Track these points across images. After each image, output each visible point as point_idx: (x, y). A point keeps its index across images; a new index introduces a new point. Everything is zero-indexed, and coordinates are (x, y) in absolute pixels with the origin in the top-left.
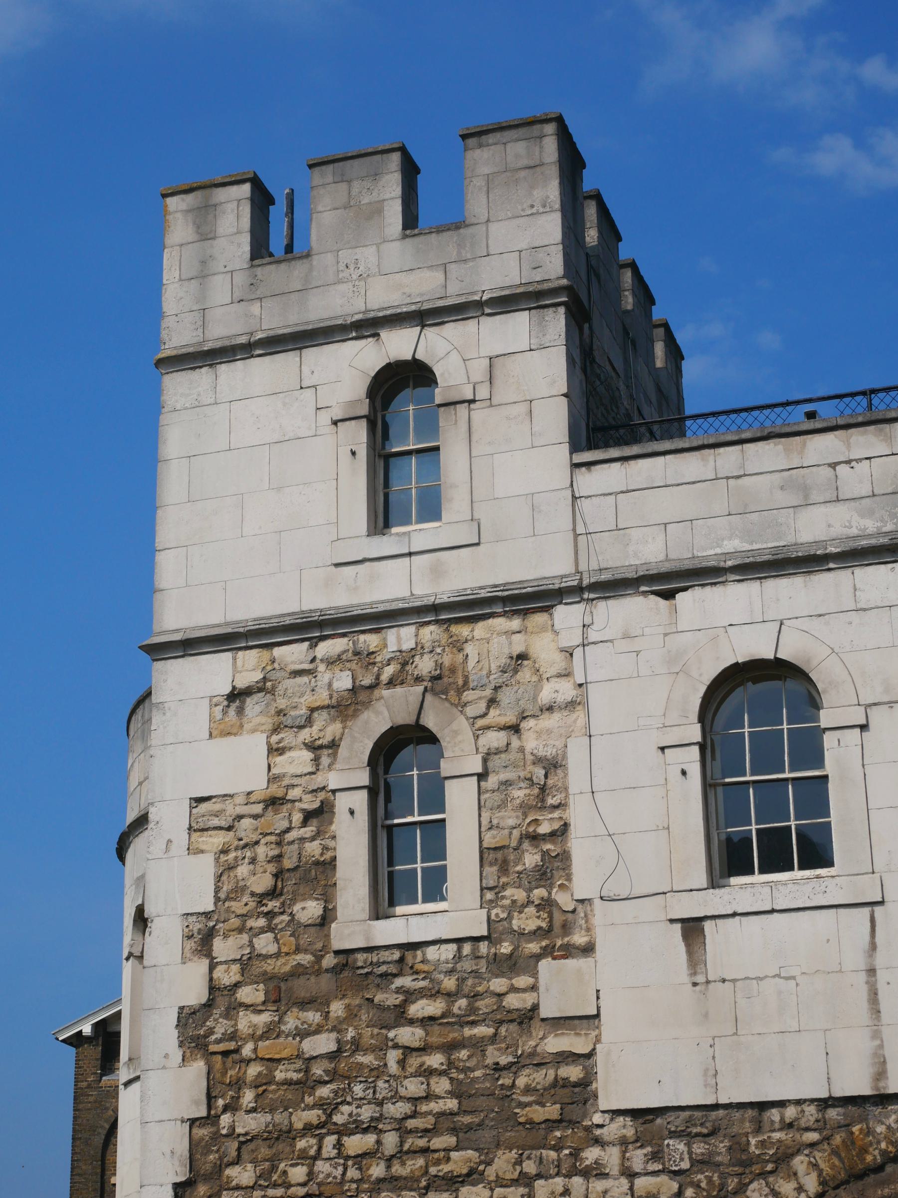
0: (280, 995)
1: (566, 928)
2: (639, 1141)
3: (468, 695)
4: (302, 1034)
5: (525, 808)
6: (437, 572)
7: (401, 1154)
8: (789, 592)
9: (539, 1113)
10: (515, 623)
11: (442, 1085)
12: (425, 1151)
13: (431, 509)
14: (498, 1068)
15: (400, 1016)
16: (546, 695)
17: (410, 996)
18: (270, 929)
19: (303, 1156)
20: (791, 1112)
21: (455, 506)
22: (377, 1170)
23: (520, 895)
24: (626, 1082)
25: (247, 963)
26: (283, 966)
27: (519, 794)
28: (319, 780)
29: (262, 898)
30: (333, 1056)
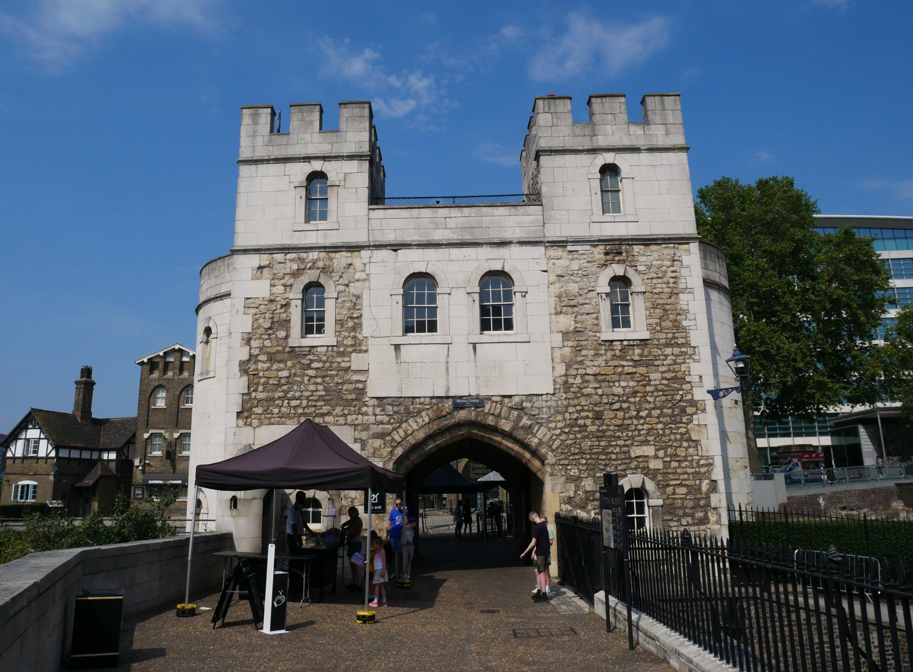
0: (272, 358)
1: (360, 345)
2: (378, 406)
3: (333, 274)
4: (278, 370)
5: (349, 309)
6: (325, 236)
7: (307, 407)
8: (430, 253)
9: (349, 397)
10: (349, 254)
11: (321, 387)
12: (315, 406)
13: (324, 216)
14: (338, 383)
15: (309, 367)
16: (357, 276)
17: (312, 361)
18: (269, 339)
19: (278, 406)
20: (422, 400)
21: (332, 217)
22: (300, 411)
23: (347, 334)
24: (375, 389)
26: (273, 350)
27: (348, 305)
28: (286, 295)
29: (267, 329)
30: (288, 377)
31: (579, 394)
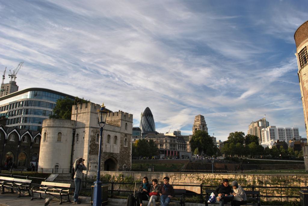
8: (110, 132)
25: (92, 143)
31: (121, 154)
